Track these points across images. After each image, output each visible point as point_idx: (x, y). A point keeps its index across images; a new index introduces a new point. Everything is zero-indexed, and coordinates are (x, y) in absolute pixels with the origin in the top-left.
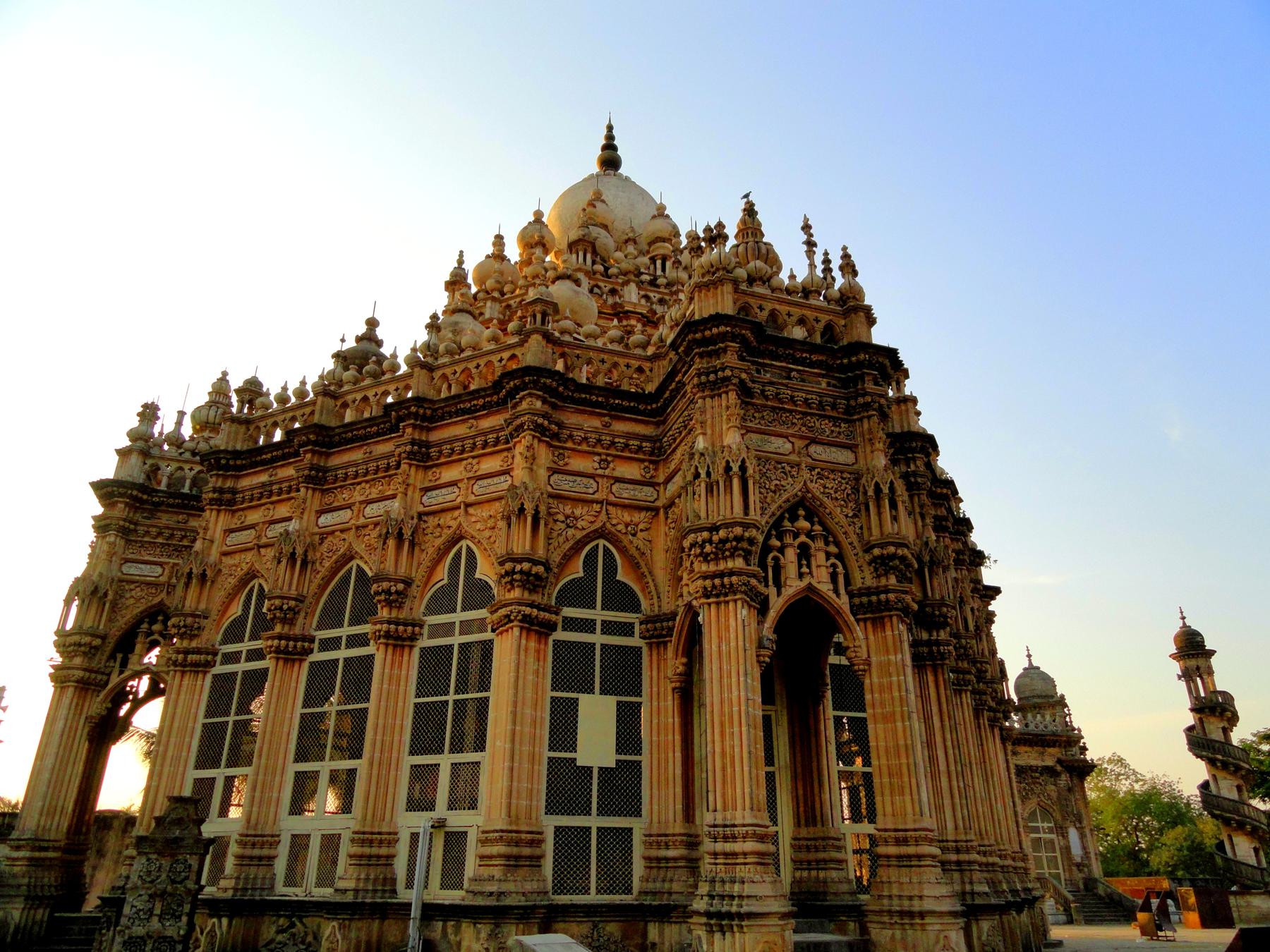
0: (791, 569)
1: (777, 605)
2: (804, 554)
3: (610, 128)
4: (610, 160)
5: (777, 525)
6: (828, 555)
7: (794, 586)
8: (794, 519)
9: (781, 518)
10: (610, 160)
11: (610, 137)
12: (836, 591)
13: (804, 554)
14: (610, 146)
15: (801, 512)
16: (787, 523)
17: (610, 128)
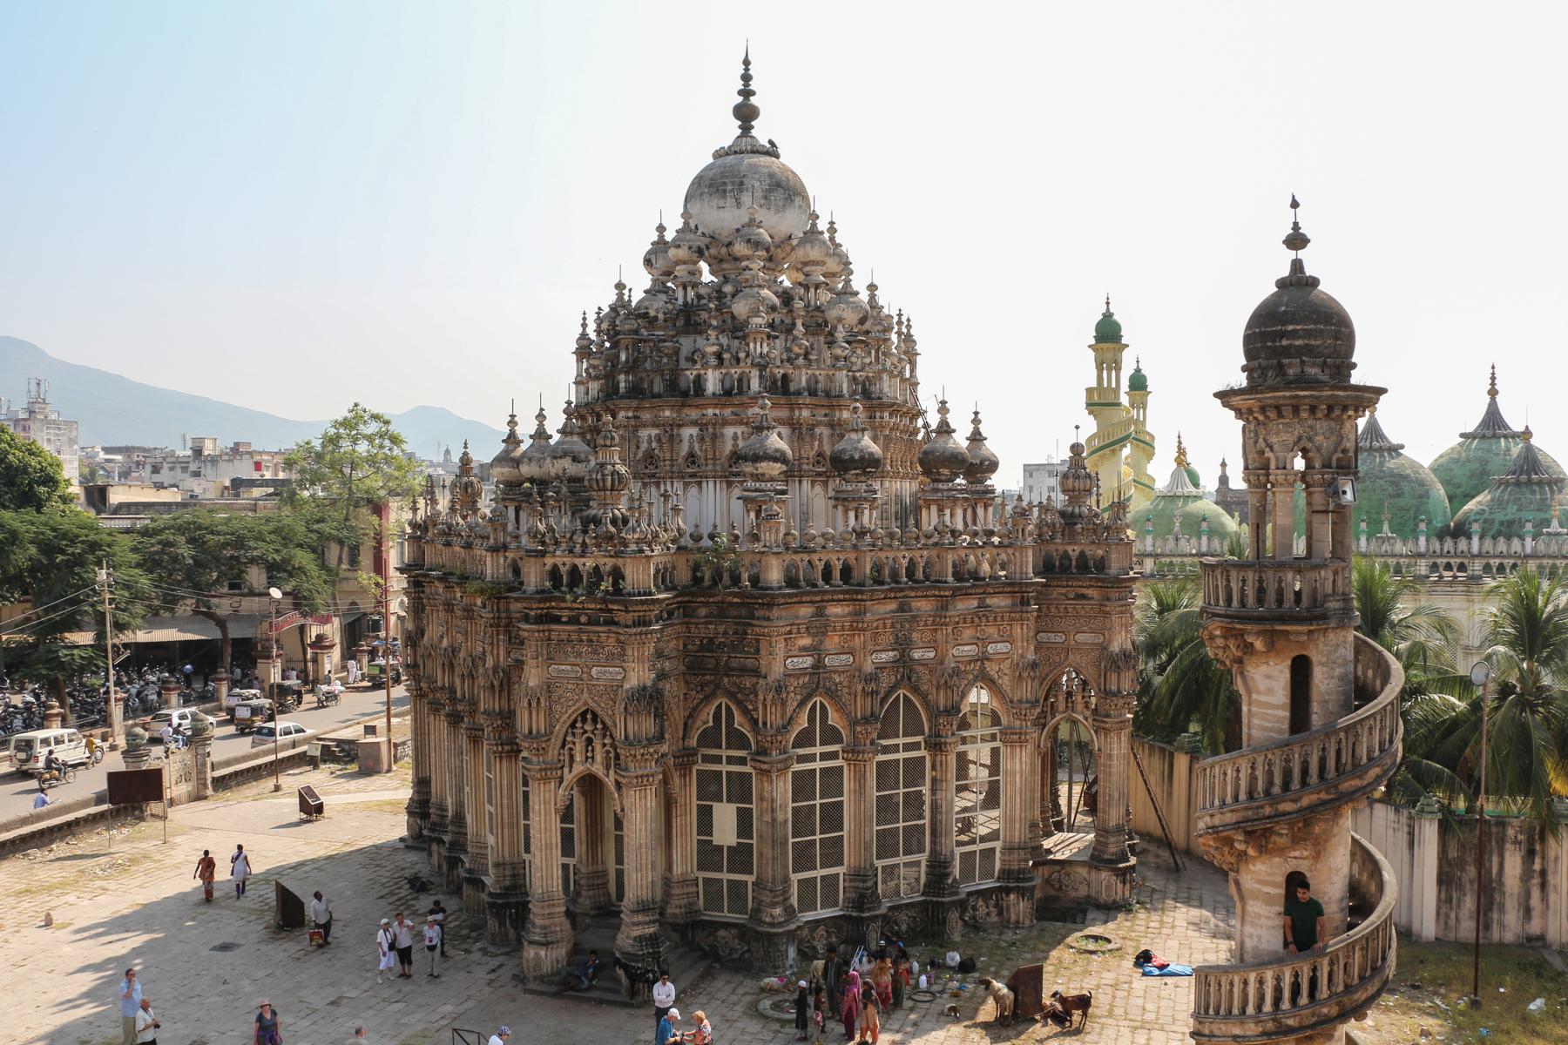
0: (578, 758)
1: (569, 777)
2: (589, 741)
3: (747, 62)
4: (746, 114)
5: (573, 726)
6: (604, 745)
7: (579, 768)
8: (584, 721)
9: (575, 721)
10: (746, 114)
11: (746, 78)
12: (608, 768)
13: (589, 741)
14: (746, 93)
15: (589, 716)
16: (579, 725)
17: (747, 62)
